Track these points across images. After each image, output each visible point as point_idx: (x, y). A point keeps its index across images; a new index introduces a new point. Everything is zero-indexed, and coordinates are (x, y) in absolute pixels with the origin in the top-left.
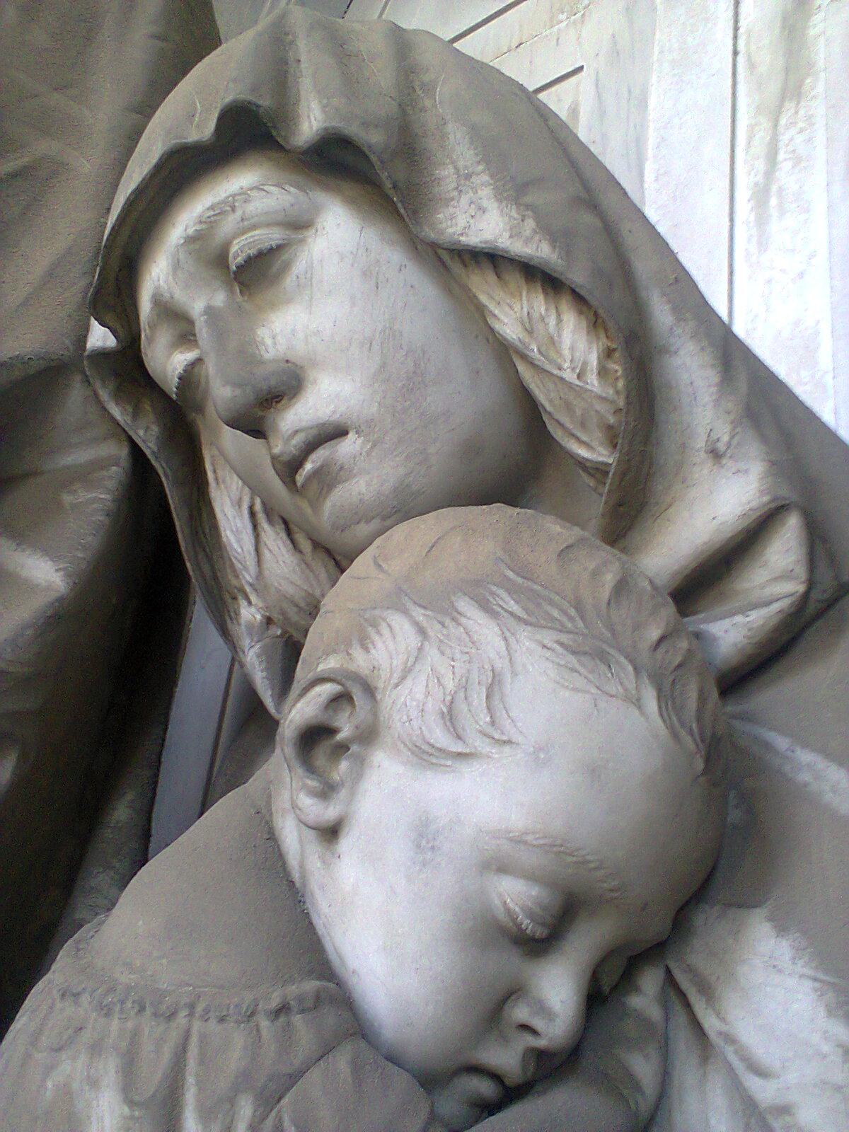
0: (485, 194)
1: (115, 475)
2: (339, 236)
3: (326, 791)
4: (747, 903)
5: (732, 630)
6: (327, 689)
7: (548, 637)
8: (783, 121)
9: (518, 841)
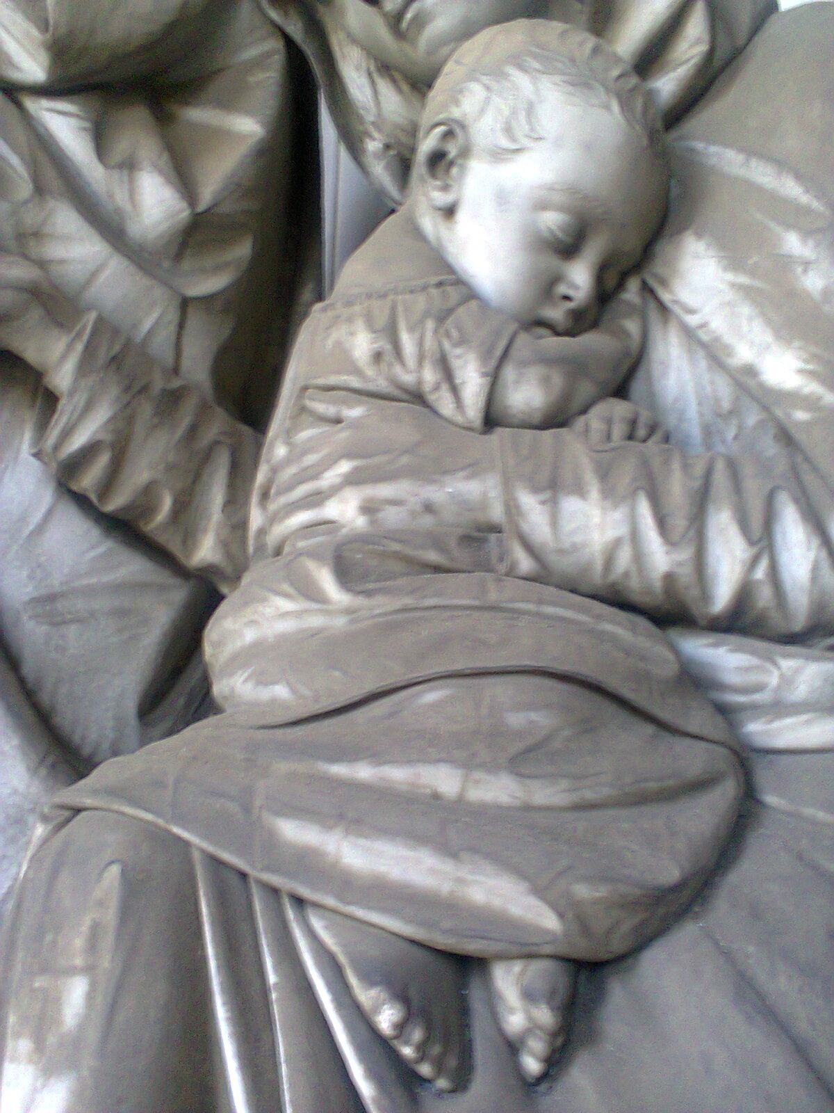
1: (278, 60)
3: (445, 188)
4: (681, 230)
5: (668, 84)
6: (440, 130)
7: (557, 79)
9: (551, 188)
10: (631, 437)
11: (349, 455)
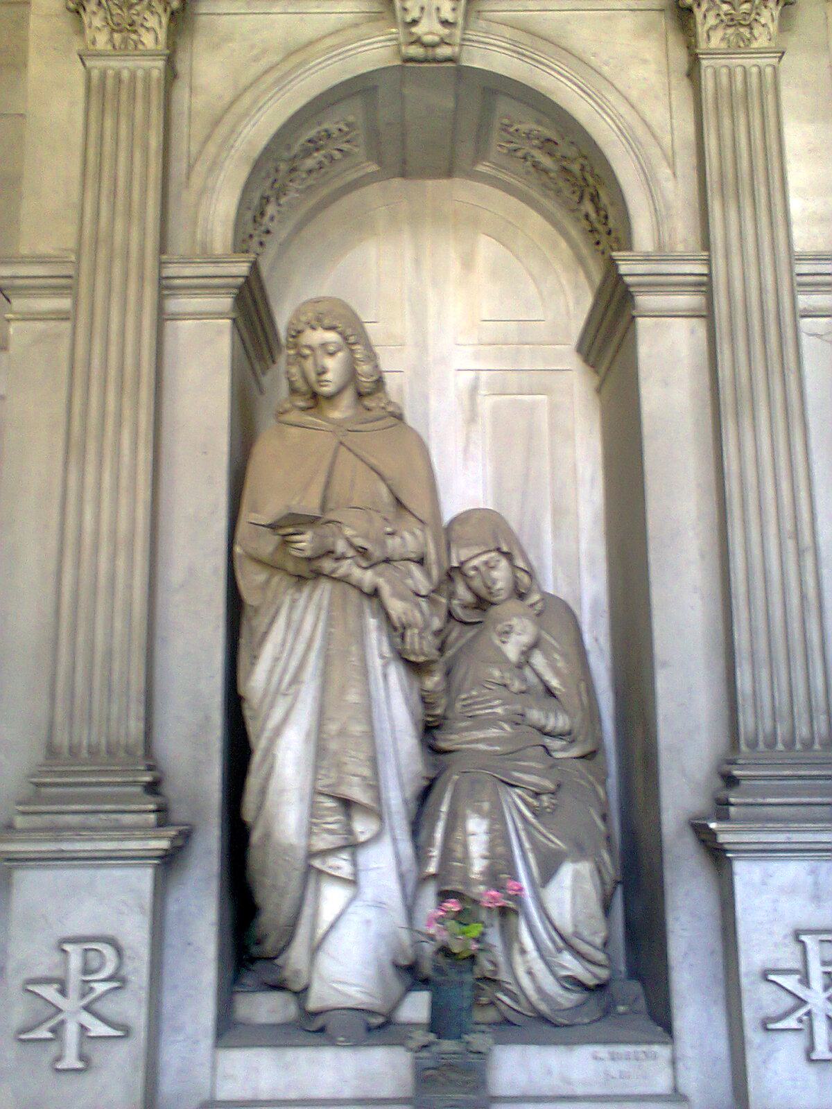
2: (504, 563)
11: (499, 699)
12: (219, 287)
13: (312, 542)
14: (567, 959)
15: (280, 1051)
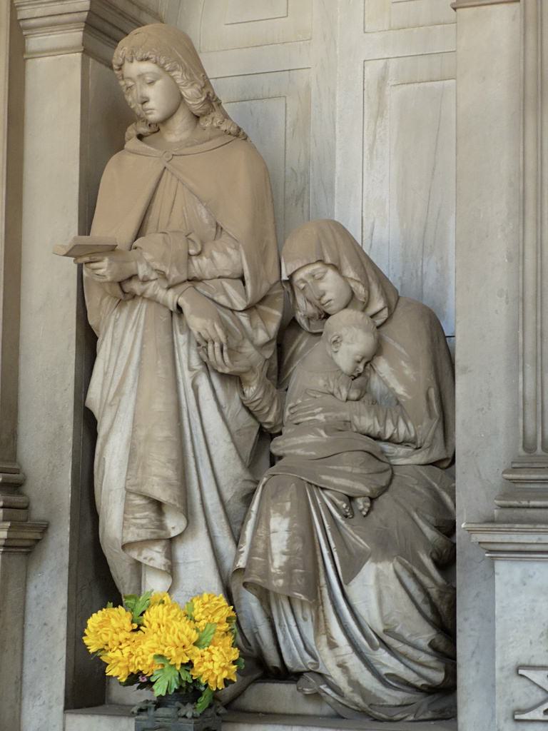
0: (350, 269)
2: (331, 274)
5: (379, 322)
8: (378, 124)
10: (372, 404)
11: (321, 407)
12: (70, 23)
13: (108, 269)
14: (382, 656)
15: (116, 719)
